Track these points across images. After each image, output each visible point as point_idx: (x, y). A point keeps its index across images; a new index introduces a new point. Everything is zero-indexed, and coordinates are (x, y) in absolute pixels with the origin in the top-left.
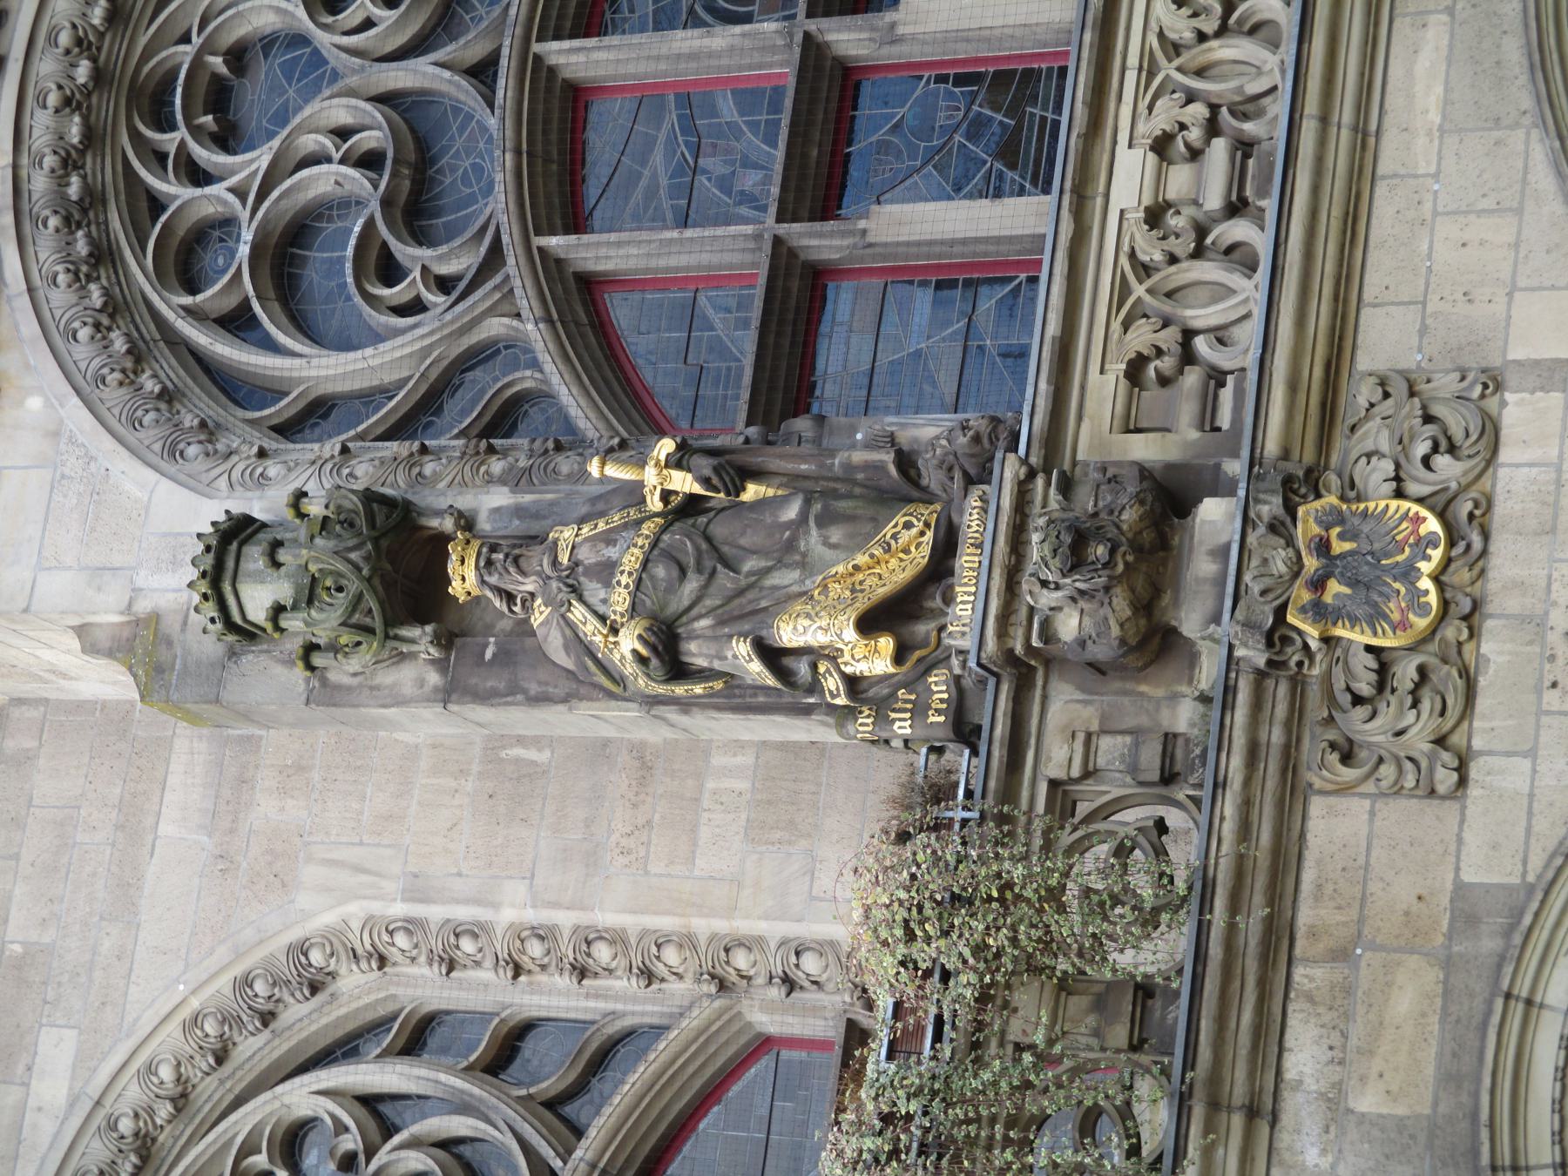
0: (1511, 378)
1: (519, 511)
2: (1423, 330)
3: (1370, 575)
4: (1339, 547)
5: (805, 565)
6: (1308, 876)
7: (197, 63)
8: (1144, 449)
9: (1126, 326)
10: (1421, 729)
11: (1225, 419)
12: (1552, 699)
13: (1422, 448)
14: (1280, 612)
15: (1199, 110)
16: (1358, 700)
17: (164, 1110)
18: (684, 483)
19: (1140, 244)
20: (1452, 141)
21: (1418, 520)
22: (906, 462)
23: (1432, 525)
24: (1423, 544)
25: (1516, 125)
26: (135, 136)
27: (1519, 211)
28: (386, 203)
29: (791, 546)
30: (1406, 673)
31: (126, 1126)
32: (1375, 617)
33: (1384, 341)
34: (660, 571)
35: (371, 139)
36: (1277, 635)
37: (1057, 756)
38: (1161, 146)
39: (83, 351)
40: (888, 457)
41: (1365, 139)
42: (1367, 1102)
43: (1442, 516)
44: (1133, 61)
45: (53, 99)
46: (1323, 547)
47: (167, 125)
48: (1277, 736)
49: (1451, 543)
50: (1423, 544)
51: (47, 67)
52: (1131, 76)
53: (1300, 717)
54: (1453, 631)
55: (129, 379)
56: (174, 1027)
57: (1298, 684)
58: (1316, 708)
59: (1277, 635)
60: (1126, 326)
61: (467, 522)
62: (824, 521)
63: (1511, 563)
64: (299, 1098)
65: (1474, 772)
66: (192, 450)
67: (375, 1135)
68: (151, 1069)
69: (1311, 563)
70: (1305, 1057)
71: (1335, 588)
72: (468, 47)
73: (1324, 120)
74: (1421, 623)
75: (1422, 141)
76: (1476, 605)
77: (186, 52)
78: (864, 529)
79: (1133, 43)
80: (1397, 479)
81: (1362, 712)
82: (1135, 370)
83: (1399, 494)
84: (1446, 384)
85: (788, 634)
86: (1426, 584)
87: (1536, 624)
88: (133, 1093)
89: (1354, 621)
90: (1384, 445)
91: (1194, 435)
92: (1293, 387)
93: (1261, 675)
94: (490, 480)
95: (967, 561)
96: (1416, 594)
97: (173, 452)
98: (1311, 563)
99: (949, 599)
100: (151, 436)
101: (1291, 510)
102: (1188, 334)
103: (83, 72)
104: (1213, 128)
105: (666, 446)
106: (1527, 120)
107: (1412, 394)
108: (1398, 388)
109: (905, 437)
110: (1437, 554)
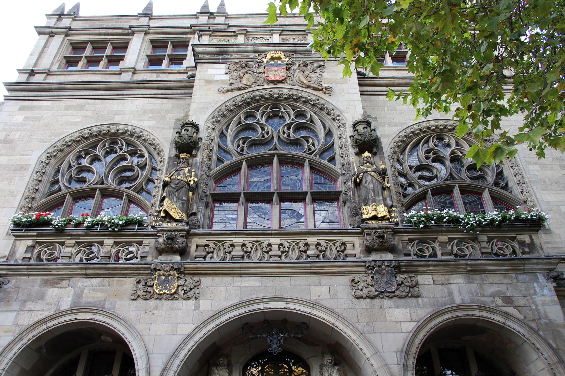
0: (197, 301)
1: (196, 163)
2: (207, 287)
3: (165, 283)
4: (170, 277)
5: (177, 201)
6: (122, 279)
7: (280, 111)
8: (193, 247)
9: (214, 243)
10: (140, 293)
11: (197, 259)
12: (144, 312)
13: (185, 288)
14: (159, 270)
15: (249, 250)
16: (146, 283)
17: (143, 138)
18: (192, 183)
19: (227, 244)
20: (239, 288)
21: (174, 289)
22: (194, 214)
23: (173, 291)
24: (170, 290)
25: (240, 298)
26: (270, 105)
27: (225, 300)
28: (254, 139)
29: (179, 199)
30: (150, 290)
31: (141, 134)
32: (158, 284)
33: (206, 281)
34: (177, 182)
35: (266, 136)
36: (155, 270)
37: (146, 241)
38: (244, 245)
39: (230, 103)
40: (194, 211)
41: (240, 275)
42: (86, 291)
43: (175, 293)
44: (258, 239)
45: (271, 93)
46: (169, 275)
47: (271, 109)
48: (142, 272)
49: (171, 295)
50: (170, 290)
51: (276, 91)
52: (256, 239)
53: (145, 274)
54: (156, 296)
55: (226, 110)
56: (153, 137)
57: (150, 274)
58: (144, 277)
59: (155, 270)
60: (214, 243)
61: (195, 156)
62: (183, 203)
63: (166, 304)
64: (146, 155)
65: (134, 301)
66: (214, 120)
67: (140, 166)
68: (148, 135)
69: (167, 274)
70: (95, 281)
71: (163, 278)
72: (278, 146)
73: (241, 268)
74: (157, 291)
75: (239, 283)
76: (160, 299)
77: (282, 110)
78: (182, 209)
79: (260, 238)
80: (181, 285)
81: (144, 283)
82: (207, 245)
83: (178, 286)
84: (196, 291)
85: (166, 200)
86: (164, 291)
87: (156, 308)
88: (145, 133)
89: (158, 281)
90: (187, 283)
91: (194, 255)
92: (197, 268)
93: (149, 268)
94: (203, 159)
95: (173, 224)
96: (162, 290)
97: (213, 117)
98: (167, 274)
99: (168, 222)
100: (216, 114)
101: (175, 269)
102: (212, 253)
103: (276, 96)
104: (246, 252)
105: (196, 179)
106: (241, 300)
107: (195, 286)
108: (198, 284)
109: (199, 214)
110: (168, 292)
